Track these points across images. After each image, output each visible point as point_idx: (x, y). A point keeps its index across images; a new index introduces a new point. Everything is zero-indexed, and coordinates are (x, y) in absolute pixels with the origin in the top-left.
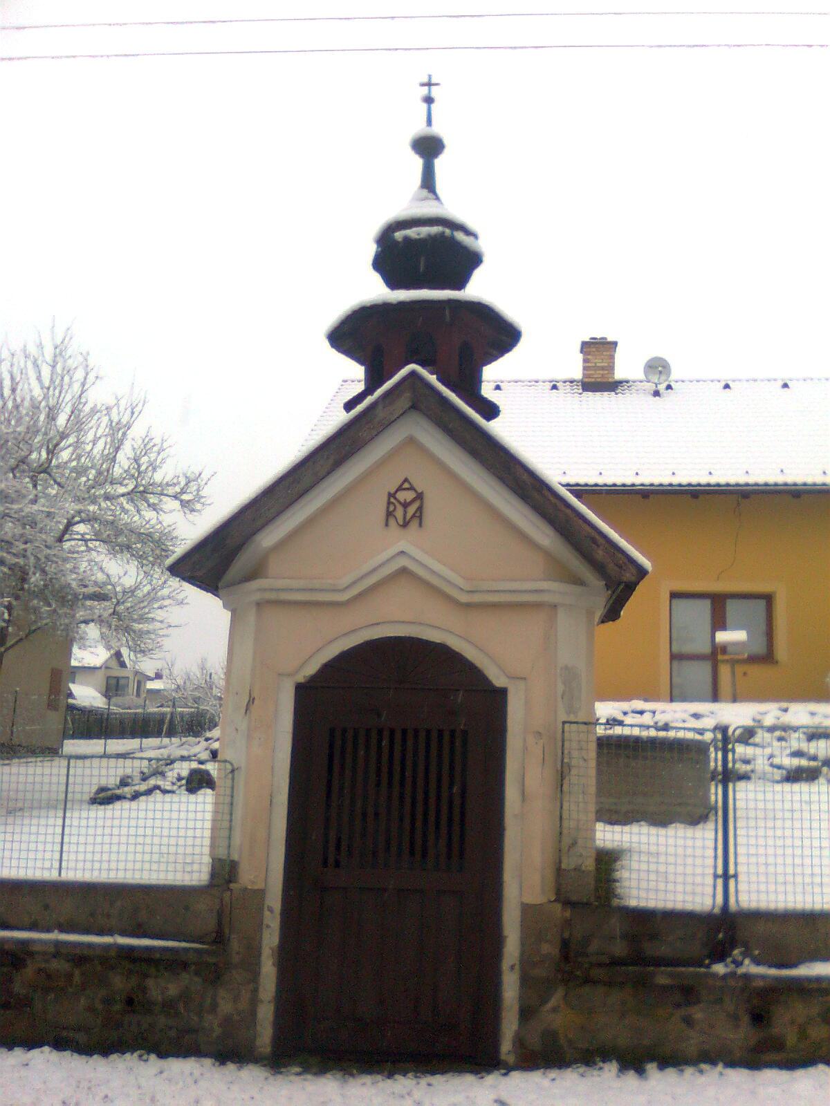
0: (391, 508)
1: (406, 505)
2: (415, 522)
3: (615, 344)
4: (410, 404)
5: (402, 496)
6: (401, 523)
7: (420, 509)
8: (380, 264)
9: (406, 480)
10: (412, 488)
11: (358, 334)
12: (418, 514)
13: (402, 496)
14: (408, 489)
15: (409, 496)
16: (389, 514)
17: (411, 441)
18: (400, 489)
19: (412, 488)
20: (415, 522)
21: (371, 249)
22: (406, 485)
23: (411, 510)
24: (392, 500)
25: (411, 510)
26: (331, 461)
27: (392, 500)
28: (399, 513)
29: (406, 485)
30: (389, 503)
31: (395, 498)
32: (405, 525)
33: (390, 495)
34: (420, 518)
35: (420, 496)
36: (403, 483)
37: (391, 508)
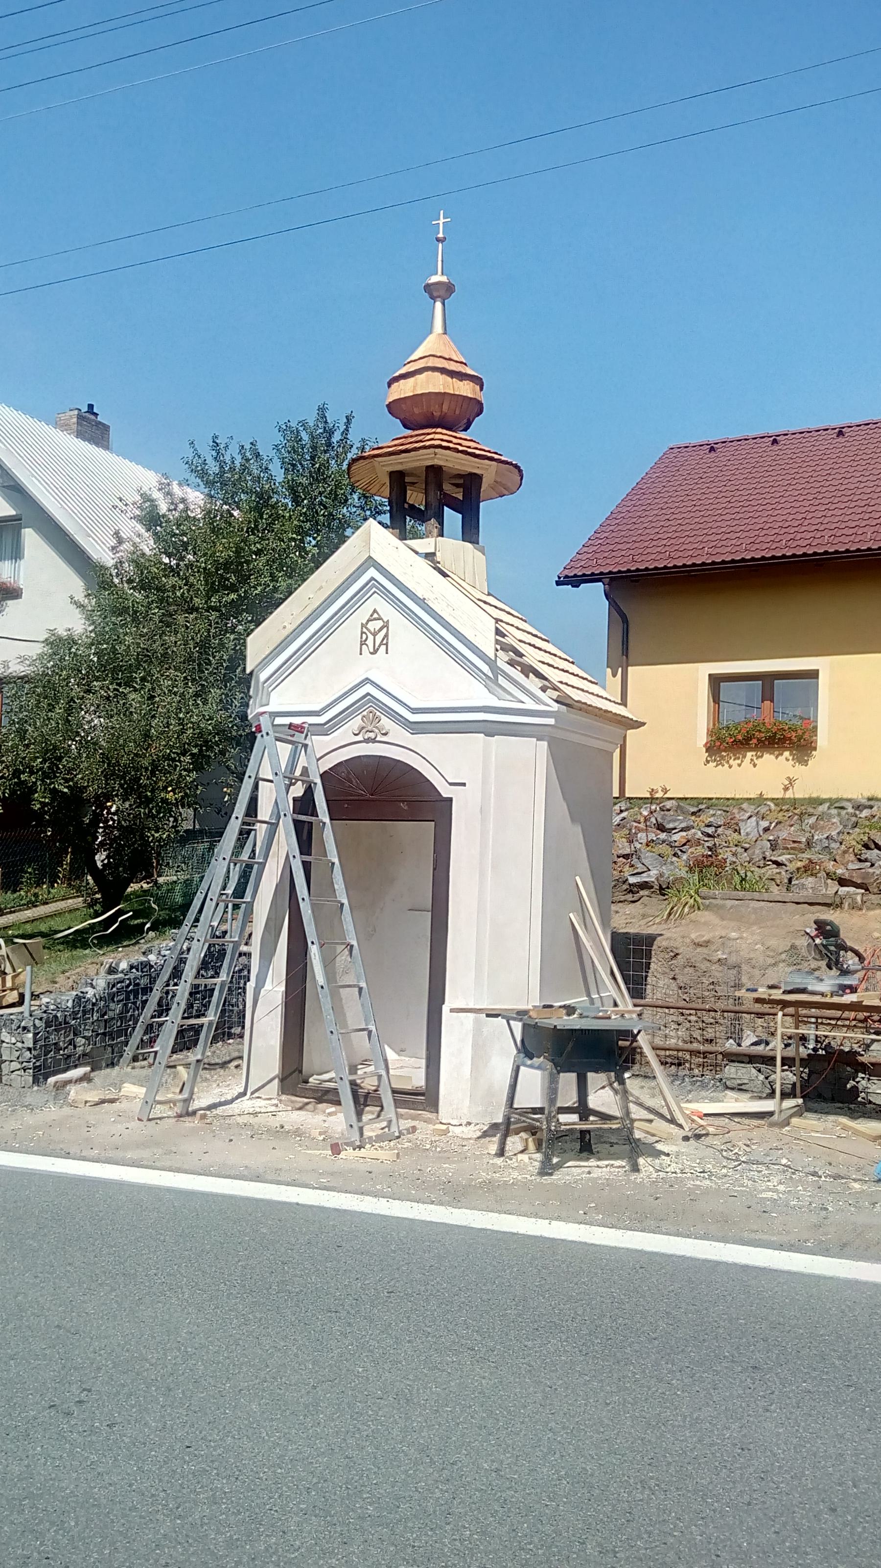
0: (364, 636)
2: (383, 648)
5: (371, 626)
6: (372, 650)
7: (386, 636)
9: (375, 611)
10: (380, 619)
12: (385, 642)
13: (375, 625)
14: (375, 619)
15: (380, 624)
16: (363, 643)
19: (380, 619)
20: (383, 648)
24: (365, 630)
27: (365, 630)
28: (370, 642)
29: (375, 616)
30: (362, 633)
32: (375, 652)
34: (387, 644)
35: (386, 625)
37: (364, 636)
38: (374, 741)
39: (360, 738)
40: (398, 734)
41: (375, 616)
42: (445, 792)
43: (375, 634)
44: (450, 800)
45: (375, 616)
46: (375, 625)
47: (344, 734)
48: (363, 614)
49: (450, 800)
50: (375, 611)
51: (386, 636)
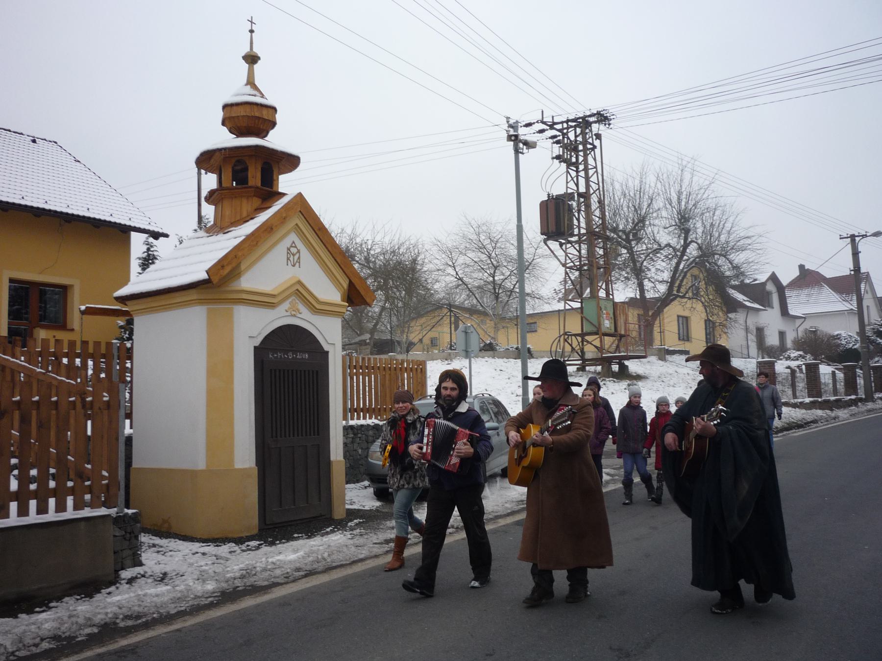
1: (294, 255)
7: (299, 258)
16: (288, 259)
23: (296, 257)
25: (296, 257)
28: (291, 259)
32: (294, 266)
33: (289, 249)
35: (299, 251)
38: (294, 316)
39: (288, 314)
40: (305, 313)
41: (293, 245)
42: (326, 347)
43: (294, 255)
44: (327, 352)
45: (293, 245)
46: (294, 250)
47: (282, 310)
48: (287, 242)
49: (327, 352)
51: (299, 258)
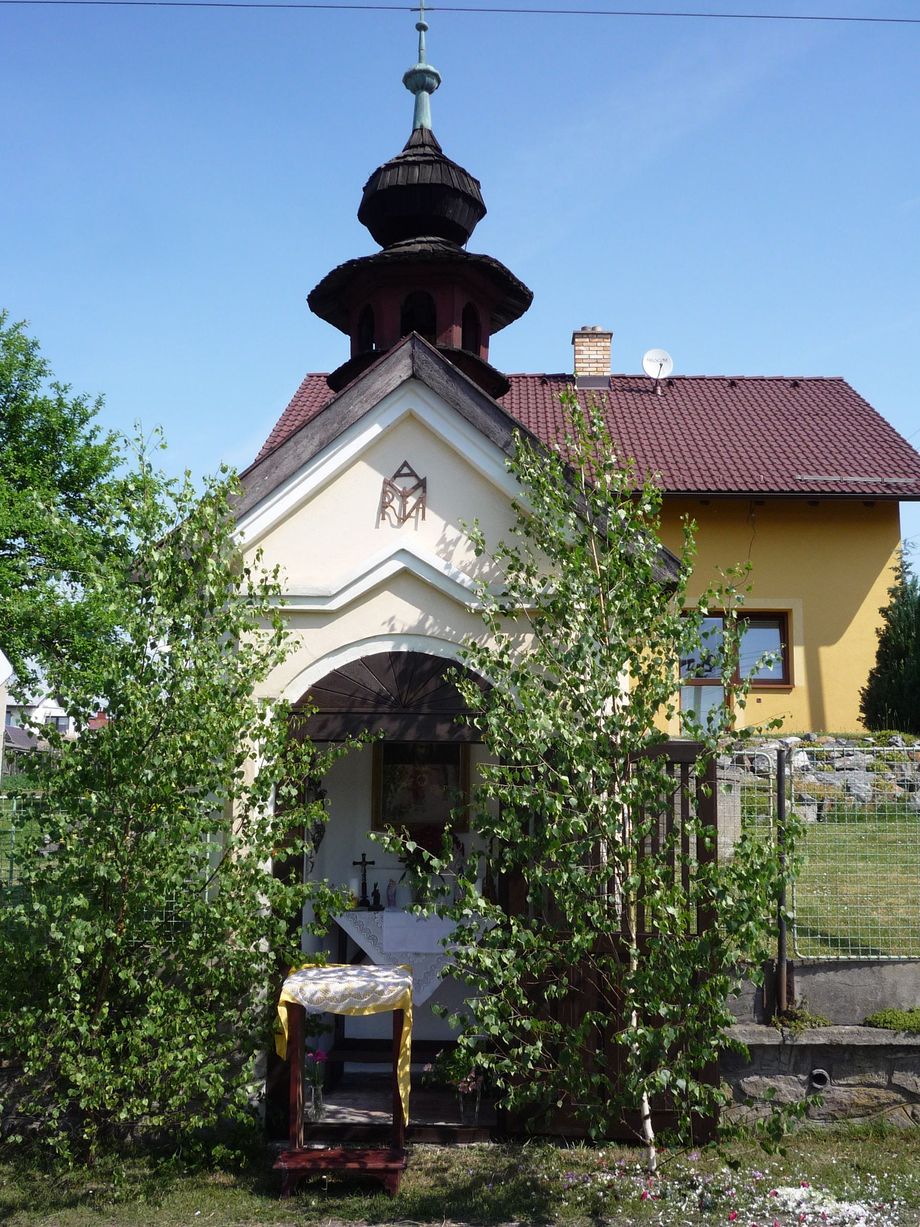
3: (611, 335)
4: (410, 372)
8: (367, 215)
9: (406, 464)
11: (335, 298)
15: (411, 482)
17: (411, 417)
18: (398, 475)
19: (412, 474)
21: (358, 197)
22: (406, 470)
25: (412, 501)
26: (316, 441)
29: (406, 470)
30: (384, 492)
31: (392, 486)
35: (422, 484)
36: (402, 467)
43: (404, 496)
50: (406, 464)
